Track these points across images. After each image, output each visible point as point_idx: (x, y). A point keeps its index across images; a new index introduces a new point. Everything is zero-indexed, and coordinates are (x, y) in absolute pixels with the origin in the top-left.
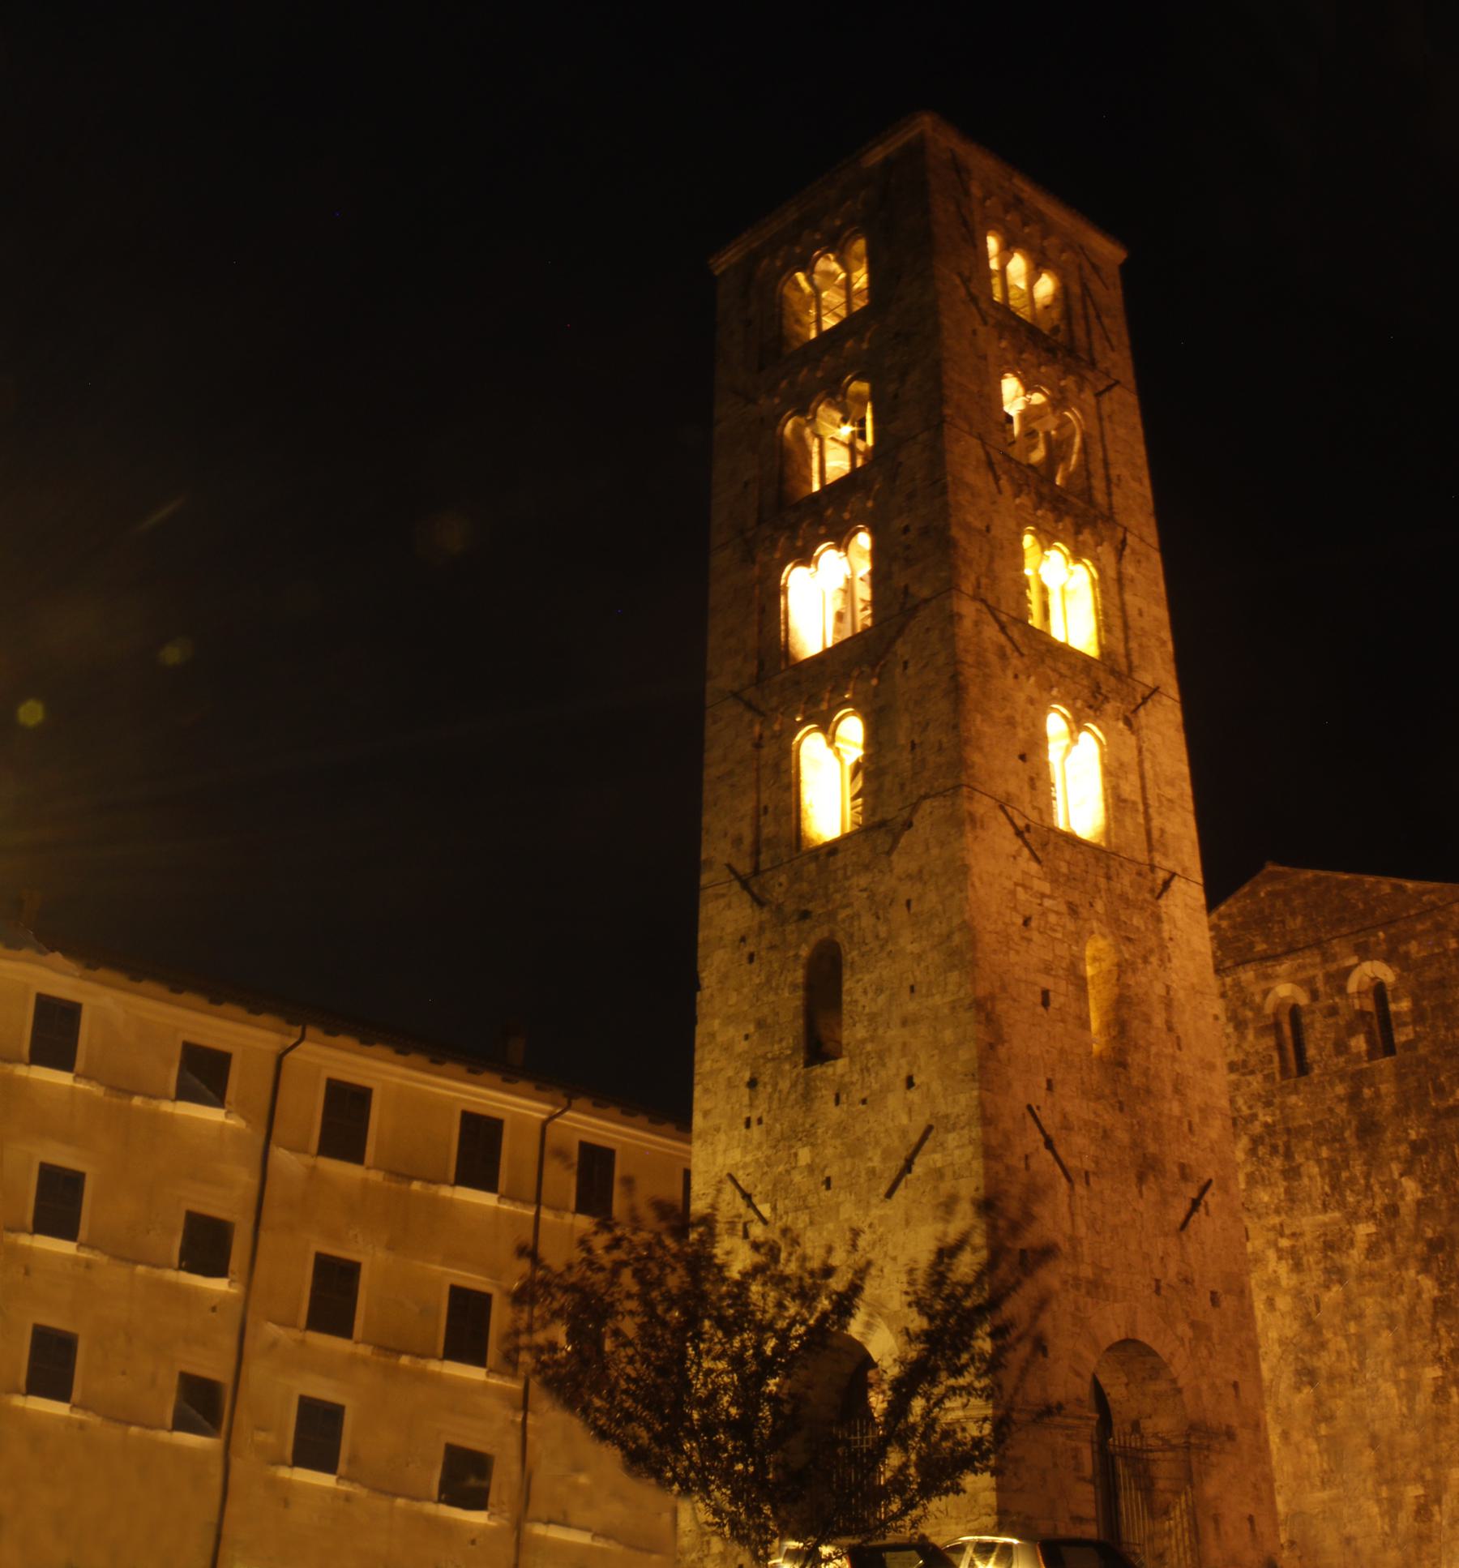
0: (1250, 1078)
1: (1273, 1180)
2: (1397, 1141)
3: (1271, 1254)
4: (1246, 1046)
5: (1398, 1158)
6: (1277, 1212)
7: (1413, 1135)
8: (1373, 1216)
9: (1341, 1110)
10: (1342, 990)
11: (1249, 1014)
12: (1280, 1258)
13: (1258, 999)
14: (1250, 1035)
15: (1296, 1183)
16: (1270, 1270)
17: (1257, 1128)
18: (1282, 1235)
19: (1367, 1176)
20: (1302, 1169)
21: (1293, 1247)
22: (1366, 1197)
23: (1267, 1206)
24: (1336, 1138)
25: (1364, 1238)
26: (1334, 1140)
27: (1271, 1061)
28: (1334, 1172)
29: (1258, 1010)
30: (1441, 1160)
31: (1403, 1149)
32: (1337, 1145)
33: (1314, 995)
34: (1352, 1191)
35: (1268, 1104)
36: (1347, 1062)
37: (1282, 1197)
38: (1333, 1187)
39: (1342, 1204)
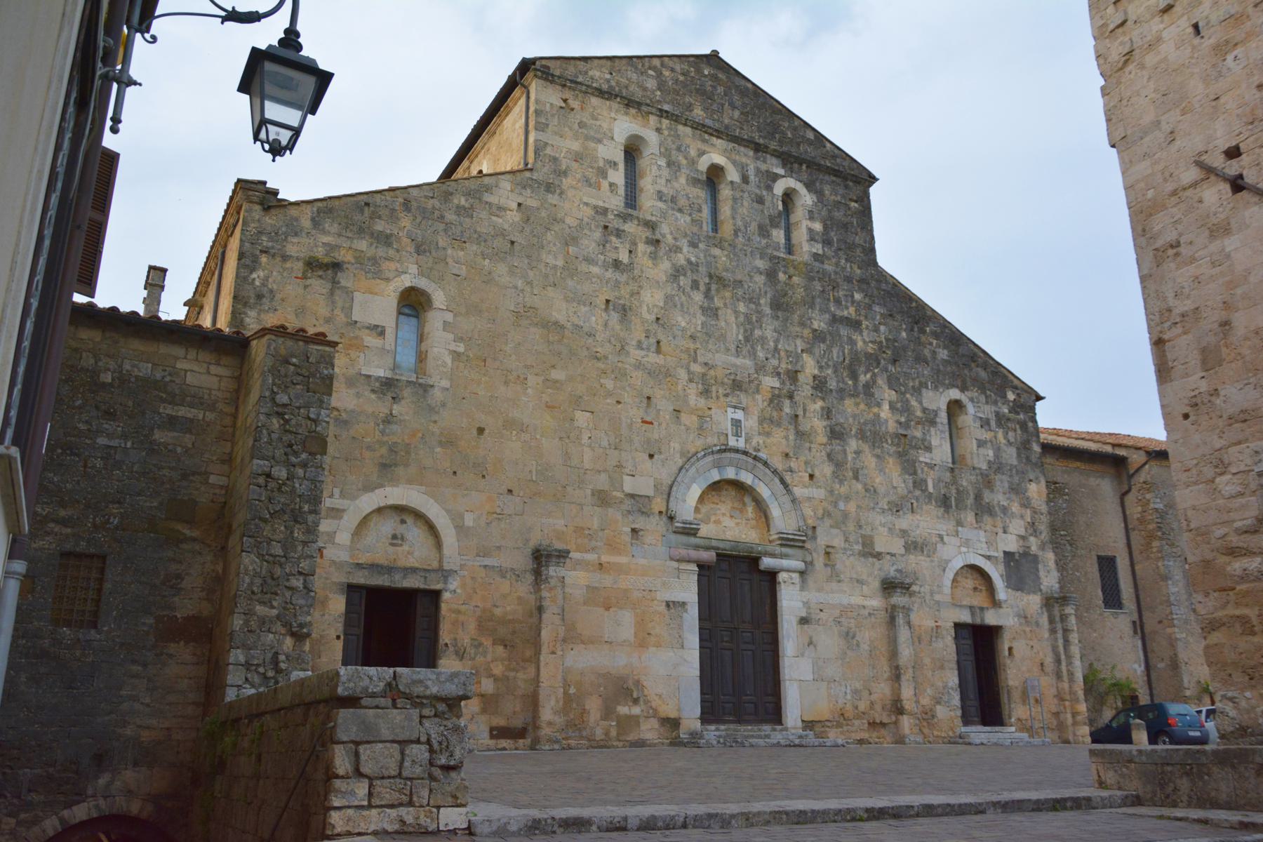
0: (679, 215)
1: (692, 311)
2: (802, 324)
3: (683, 374)
4: (676, 185)
5: (802, 337)
6: (693, 337)
7: (816, 326)
8: (778, 374)
9: (760, 280)
10: (769, 188)
11: (684, 162)
12: (691, 380)
13: (693, 153)
14: (683, 180)
15: (713, 322)
16: (680, 387)
17: (681, 259)
18: (695, 361)
19: (777, 341)
20: (720, 312)
21: (704, 375)
22: (773, 356)
23: (684, 330)
24: (752, 300)
25: (769, 389)
26: (751, 300)
27: (700, 211)
28: (750, 324)
29: (693, 163)
30: (835, 351)
31: (806, 332)
32: (753, 306)
33: (745, 179)
34: (763, 348)
35: (693, 245)
36: (767, 246)
37: (699, 328)
38: (747, 339)
39: (753, 354)
